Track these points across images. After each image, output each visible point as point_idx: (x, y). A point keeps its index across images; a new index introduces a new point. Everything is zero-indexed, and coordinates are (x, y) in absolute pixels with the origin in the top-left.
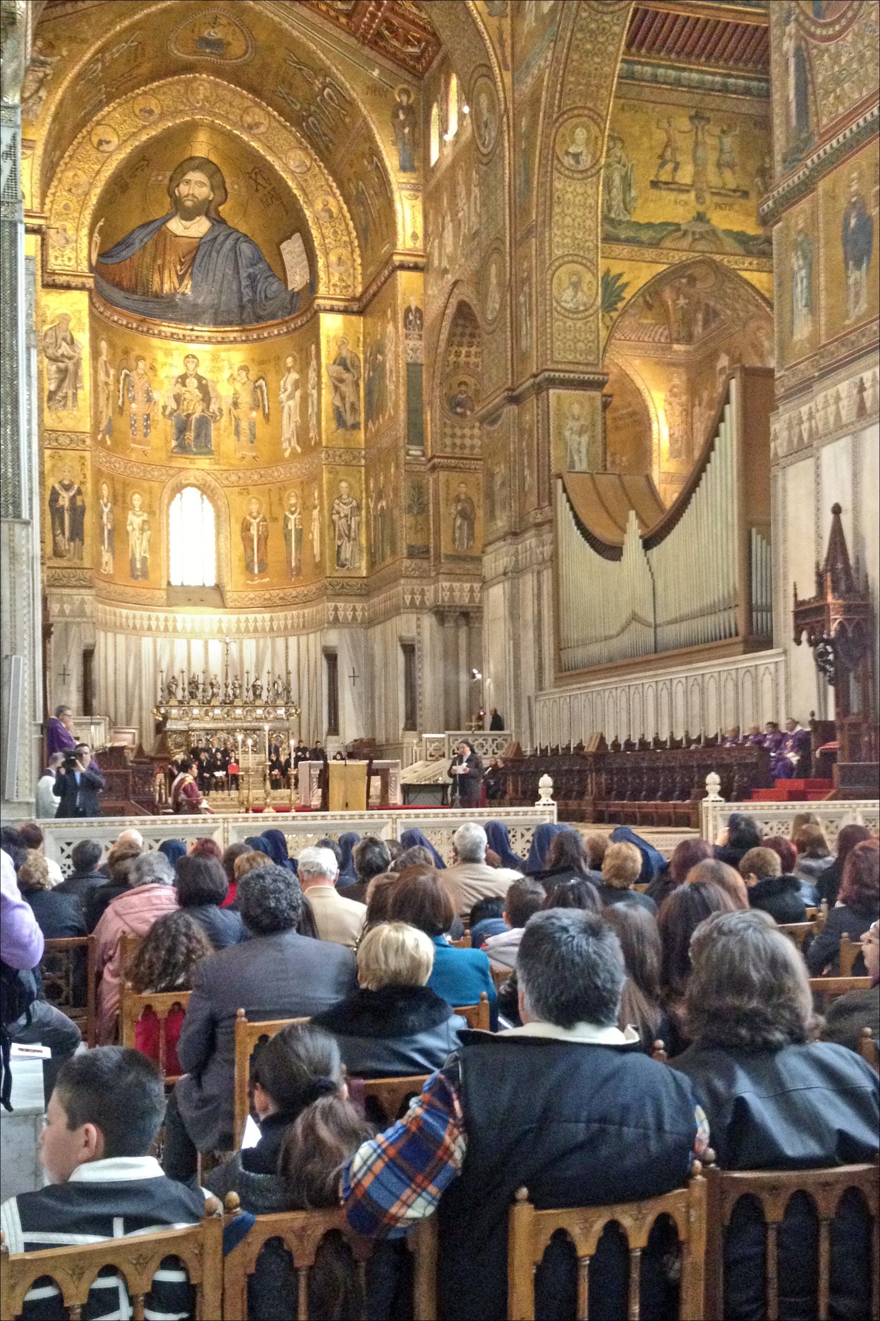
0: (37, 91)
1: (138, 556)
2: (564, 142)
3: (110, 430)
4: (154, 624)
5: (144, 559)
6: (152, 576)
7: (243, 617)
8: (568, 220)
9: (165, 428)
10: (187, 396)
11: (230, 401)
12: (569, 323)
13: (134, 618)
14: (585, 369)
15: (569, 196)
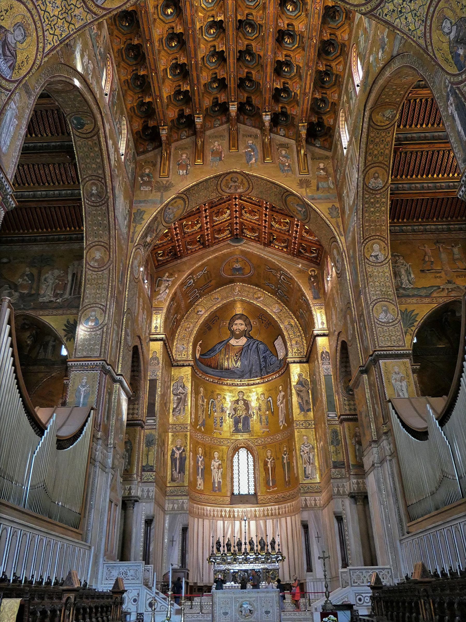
0: (165, 290)
1: (216, 481)
2: (369, 251)
3: (203, 424)
4: (223, 513)
5: (219, 482)
6: (223, 490)
7: (266, 508)
8: (377, 283)
9: (228, 422)
10: (239, 408)
11: (257, 408)
12: (386, 328)
13: (214, 511)
14: (398, 348)
15: (375, 273)
